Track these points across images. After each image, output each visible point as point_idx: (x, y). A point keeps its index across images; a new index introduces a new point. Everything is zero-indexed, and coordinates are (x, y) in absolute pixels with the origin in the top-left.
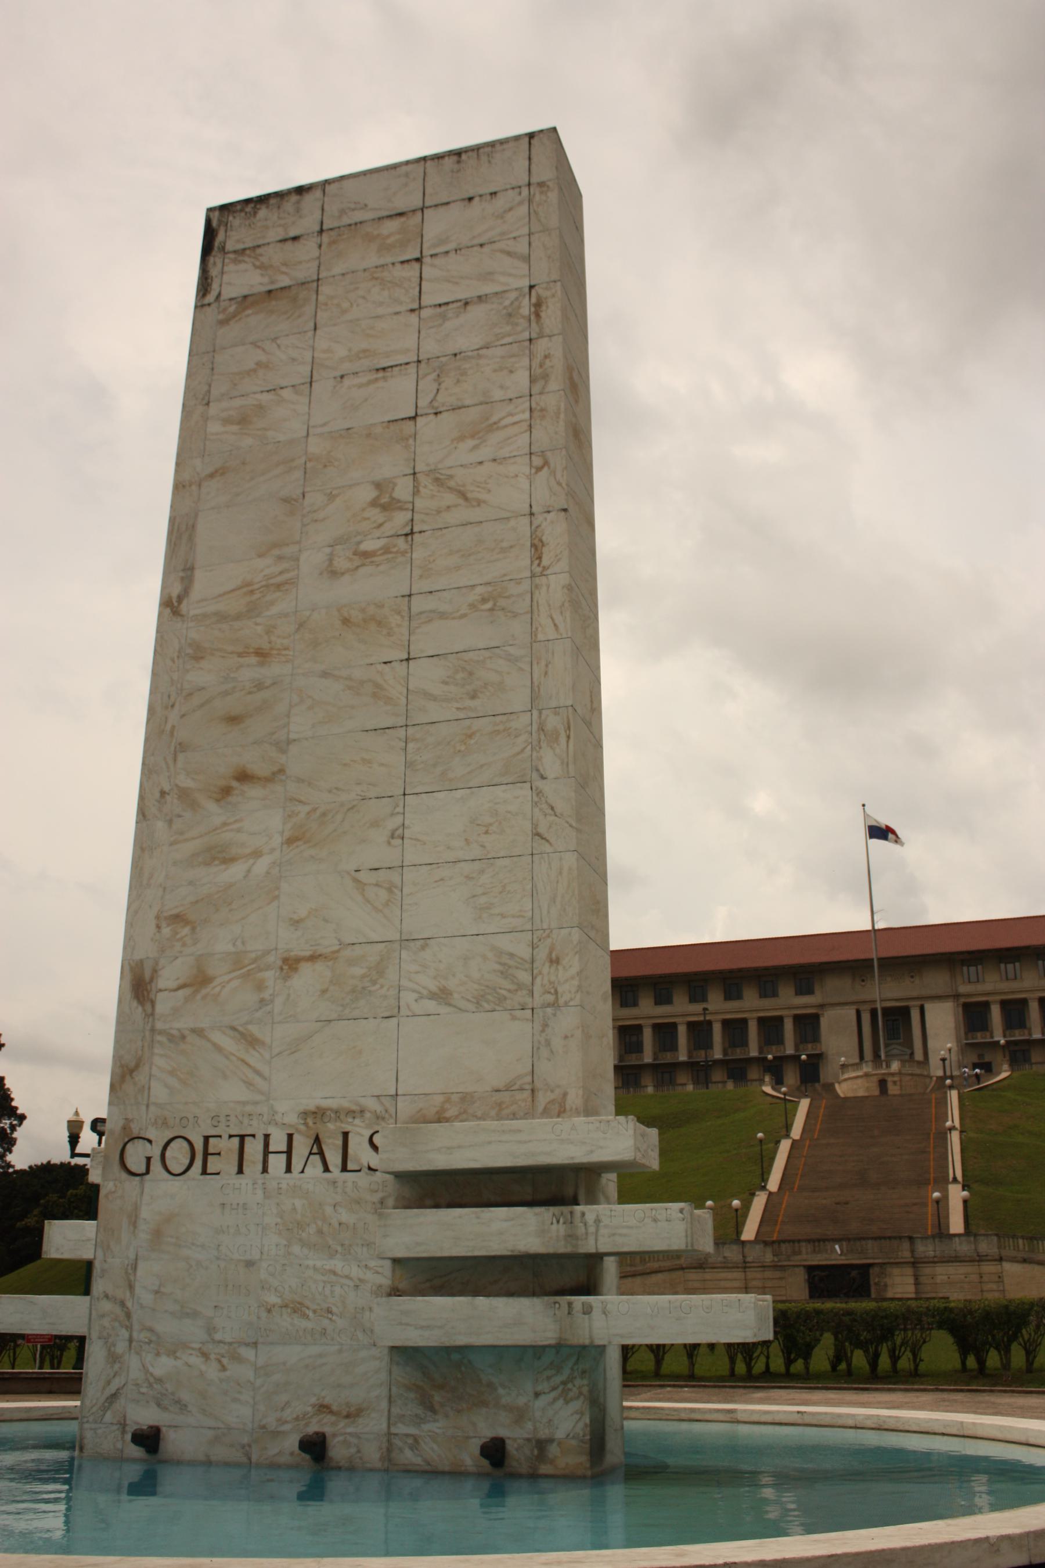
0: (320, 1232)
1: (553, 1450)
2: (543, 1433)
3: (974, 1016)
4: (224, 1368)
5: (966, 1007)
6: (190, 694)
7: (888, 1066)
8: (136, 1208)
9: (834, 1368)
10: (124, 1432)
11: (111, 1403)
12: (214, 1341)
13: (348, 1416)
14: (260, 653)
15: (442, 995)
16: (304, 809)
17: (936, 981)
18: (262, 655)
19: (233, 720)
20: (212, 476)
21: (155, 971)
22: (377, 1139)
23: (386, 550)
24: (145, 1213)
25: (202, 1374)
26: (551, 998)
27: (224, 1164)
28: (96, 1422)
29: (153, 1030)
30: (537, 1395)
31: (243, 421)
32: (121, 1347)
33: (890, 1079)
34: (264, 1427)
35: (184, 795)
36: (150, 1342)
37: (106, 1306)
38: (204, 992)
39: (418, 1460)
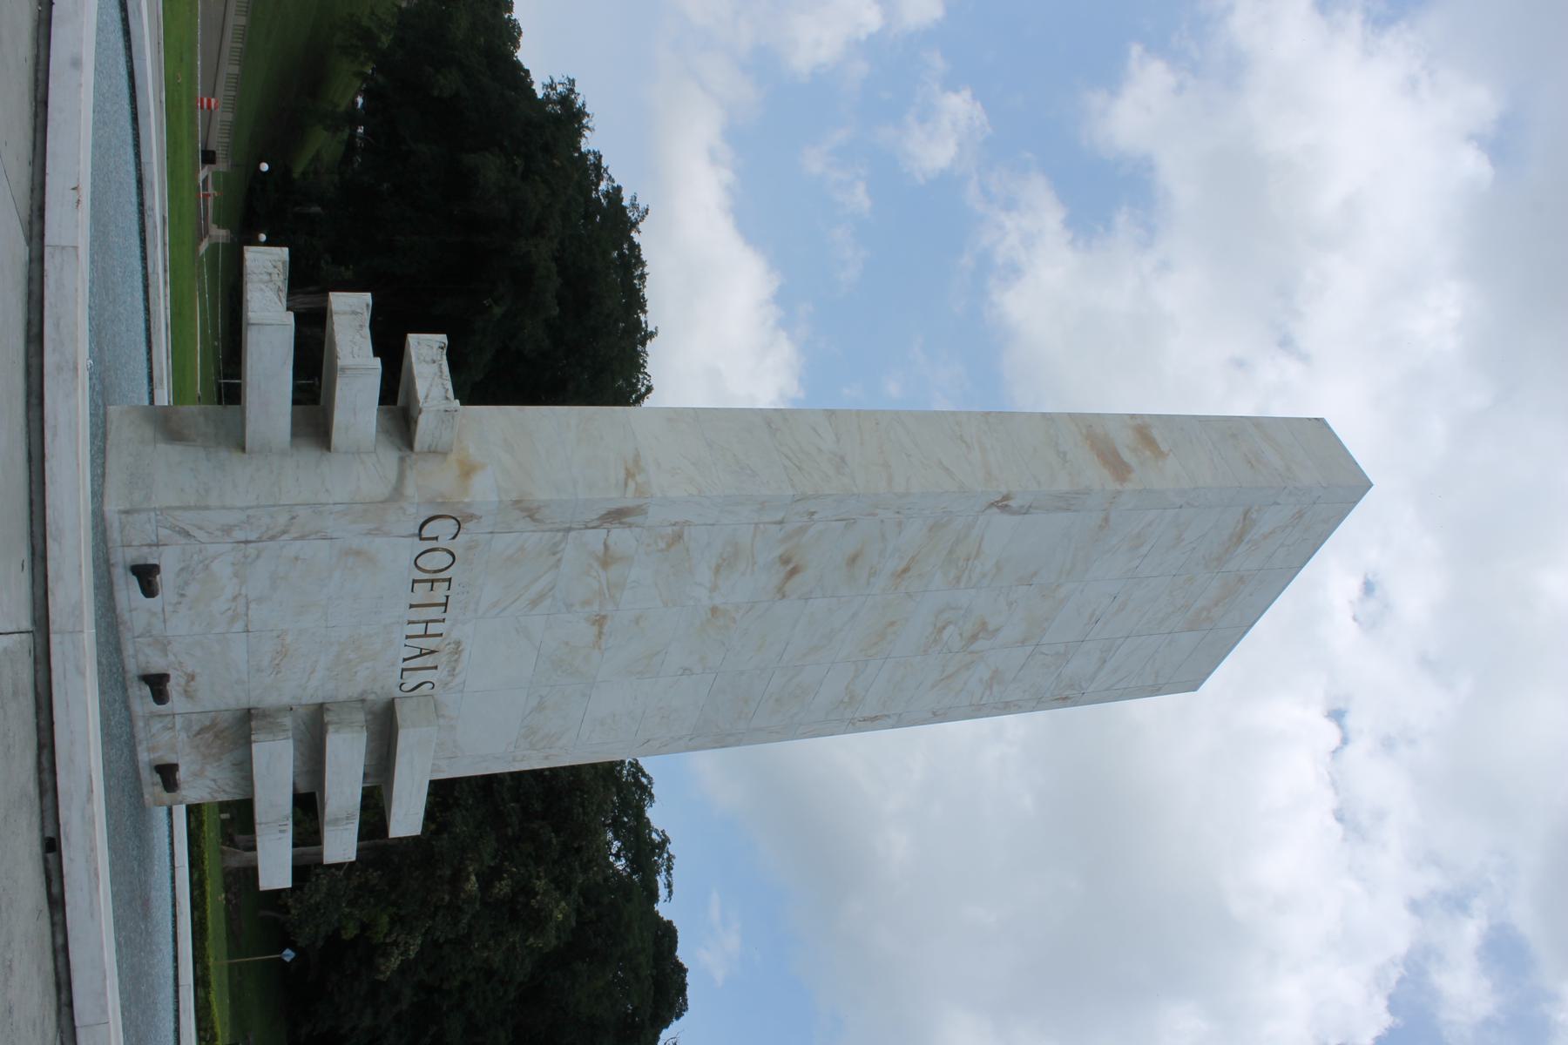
6: (900, 524)
10: (150, 545)
19: (853, 560)
20: (1106, 520)
21: (630, 526)
29: (569, 529)
36: (245, 557)
37: (283, 519)
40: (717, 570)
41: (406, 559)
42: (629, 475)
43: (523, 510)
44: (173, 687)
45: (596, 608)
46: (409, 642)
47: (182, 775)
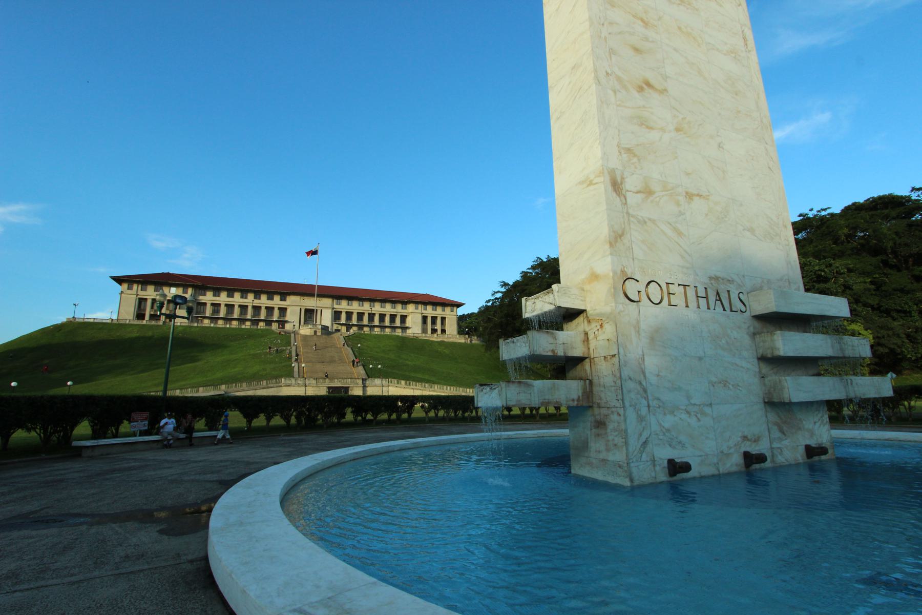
0: (727, 343)
3: (337, 315)
4: (699, 420)
8: (638, 322)
10: (654, 466)
11: (644, 448)
12: (691, 404)
13: (755, 441)
15: (751, 230)
17: (327, 302)
18: (646, 24)
19: (637, 50)
21: (623, 178)
24: (643, 326)
25: (689, 424)
28: (637, 461)
29: (628, 213)
30: (815, 423)
34: (722, 452)
35: (619, 79)
36: (659, 407)
38: (651, 198)
39: (783, 460)
40: (650, 128)
42: (591, 183)
43: (616, 241)
44: (754, 449)
45: (681, 199)
46: (712, 307)
47: (813, 443)
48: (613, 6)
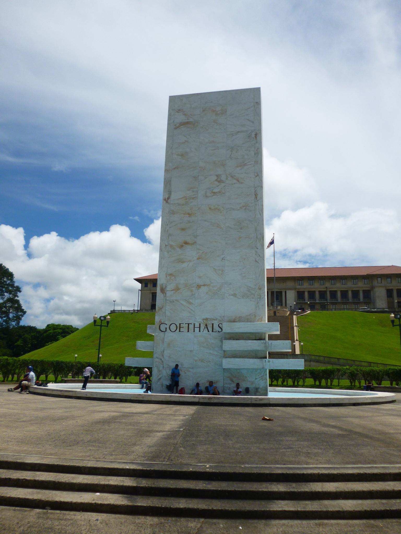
0: (207, 345)
1: (259, 390)
2: (257, 386)
3: (300, 295)
5: (298, 292)
7: (277, 308)
8: (164, 339)
9: (282, 384)
14: (189, 214)
15: (234, 295)
16: (201, 252)
17: (290, 284)
18: (189, 215)
19: (183, 229)
20: (175, 169)
21: (166, 287)
22: (220, 325)
23: (220, 192)
24: (165, 340)
26: (259, 297)
27: (185, 329)
29: (166, 300)
30: (256, 379)
31: (182, 155)
32: (161, 368)
33: (277, 311)
35: (171, 246)
37: (157, 360)
41: (173, 334)
48: (174, 214)
